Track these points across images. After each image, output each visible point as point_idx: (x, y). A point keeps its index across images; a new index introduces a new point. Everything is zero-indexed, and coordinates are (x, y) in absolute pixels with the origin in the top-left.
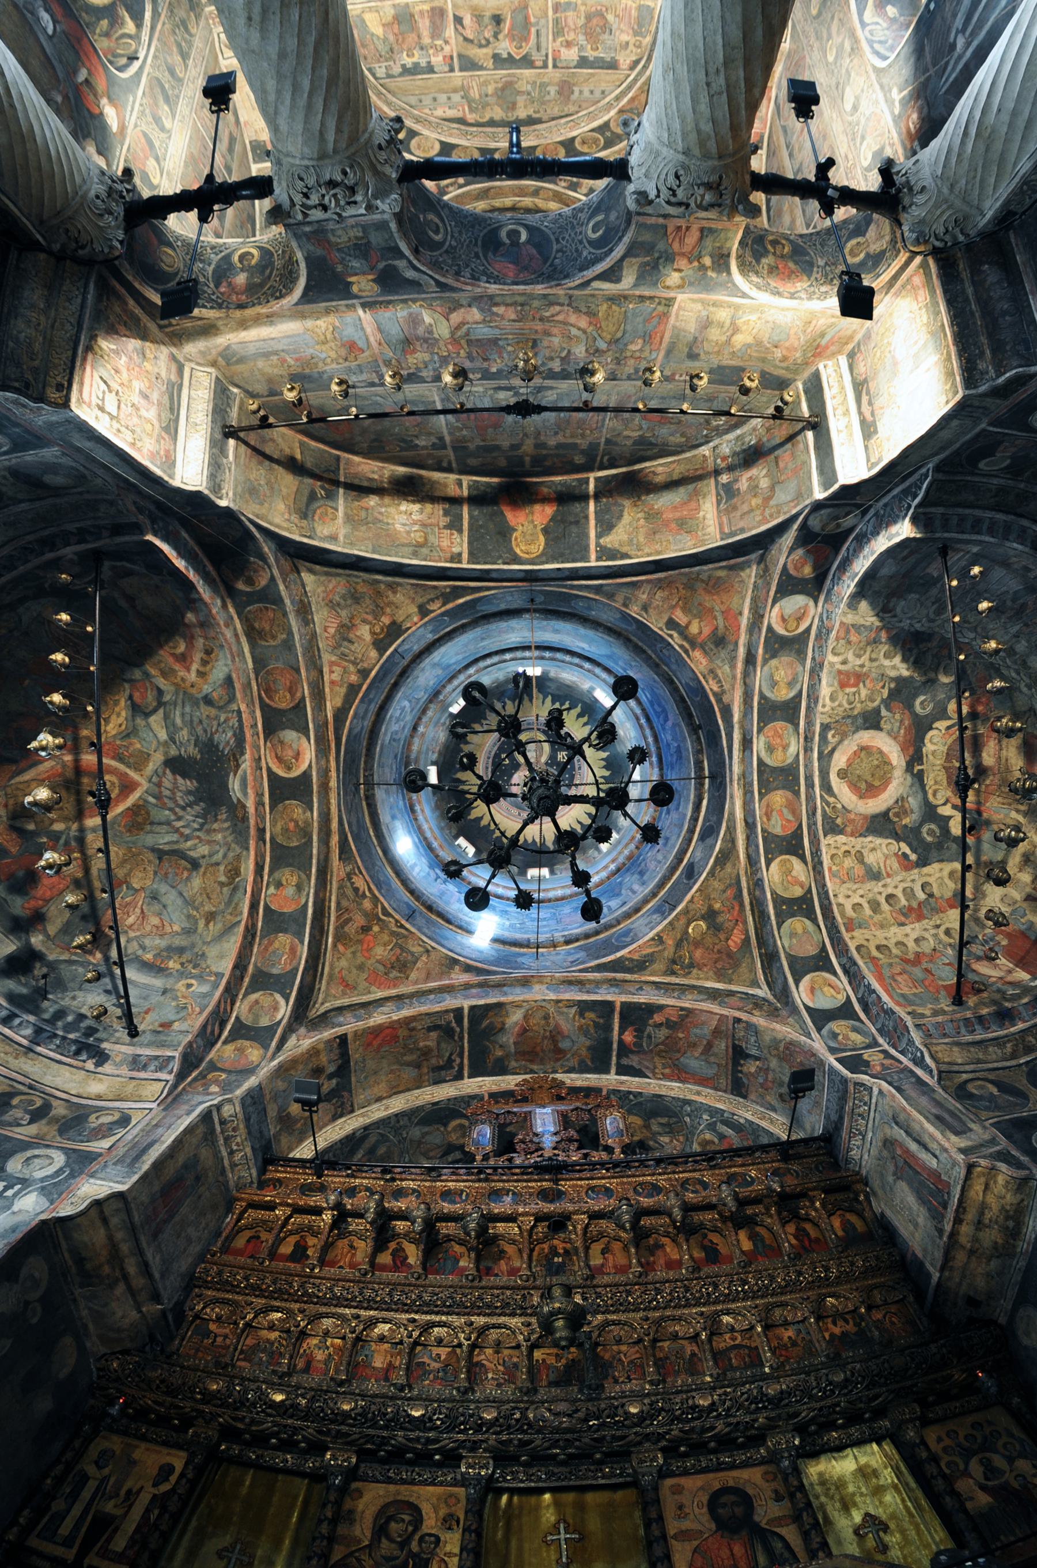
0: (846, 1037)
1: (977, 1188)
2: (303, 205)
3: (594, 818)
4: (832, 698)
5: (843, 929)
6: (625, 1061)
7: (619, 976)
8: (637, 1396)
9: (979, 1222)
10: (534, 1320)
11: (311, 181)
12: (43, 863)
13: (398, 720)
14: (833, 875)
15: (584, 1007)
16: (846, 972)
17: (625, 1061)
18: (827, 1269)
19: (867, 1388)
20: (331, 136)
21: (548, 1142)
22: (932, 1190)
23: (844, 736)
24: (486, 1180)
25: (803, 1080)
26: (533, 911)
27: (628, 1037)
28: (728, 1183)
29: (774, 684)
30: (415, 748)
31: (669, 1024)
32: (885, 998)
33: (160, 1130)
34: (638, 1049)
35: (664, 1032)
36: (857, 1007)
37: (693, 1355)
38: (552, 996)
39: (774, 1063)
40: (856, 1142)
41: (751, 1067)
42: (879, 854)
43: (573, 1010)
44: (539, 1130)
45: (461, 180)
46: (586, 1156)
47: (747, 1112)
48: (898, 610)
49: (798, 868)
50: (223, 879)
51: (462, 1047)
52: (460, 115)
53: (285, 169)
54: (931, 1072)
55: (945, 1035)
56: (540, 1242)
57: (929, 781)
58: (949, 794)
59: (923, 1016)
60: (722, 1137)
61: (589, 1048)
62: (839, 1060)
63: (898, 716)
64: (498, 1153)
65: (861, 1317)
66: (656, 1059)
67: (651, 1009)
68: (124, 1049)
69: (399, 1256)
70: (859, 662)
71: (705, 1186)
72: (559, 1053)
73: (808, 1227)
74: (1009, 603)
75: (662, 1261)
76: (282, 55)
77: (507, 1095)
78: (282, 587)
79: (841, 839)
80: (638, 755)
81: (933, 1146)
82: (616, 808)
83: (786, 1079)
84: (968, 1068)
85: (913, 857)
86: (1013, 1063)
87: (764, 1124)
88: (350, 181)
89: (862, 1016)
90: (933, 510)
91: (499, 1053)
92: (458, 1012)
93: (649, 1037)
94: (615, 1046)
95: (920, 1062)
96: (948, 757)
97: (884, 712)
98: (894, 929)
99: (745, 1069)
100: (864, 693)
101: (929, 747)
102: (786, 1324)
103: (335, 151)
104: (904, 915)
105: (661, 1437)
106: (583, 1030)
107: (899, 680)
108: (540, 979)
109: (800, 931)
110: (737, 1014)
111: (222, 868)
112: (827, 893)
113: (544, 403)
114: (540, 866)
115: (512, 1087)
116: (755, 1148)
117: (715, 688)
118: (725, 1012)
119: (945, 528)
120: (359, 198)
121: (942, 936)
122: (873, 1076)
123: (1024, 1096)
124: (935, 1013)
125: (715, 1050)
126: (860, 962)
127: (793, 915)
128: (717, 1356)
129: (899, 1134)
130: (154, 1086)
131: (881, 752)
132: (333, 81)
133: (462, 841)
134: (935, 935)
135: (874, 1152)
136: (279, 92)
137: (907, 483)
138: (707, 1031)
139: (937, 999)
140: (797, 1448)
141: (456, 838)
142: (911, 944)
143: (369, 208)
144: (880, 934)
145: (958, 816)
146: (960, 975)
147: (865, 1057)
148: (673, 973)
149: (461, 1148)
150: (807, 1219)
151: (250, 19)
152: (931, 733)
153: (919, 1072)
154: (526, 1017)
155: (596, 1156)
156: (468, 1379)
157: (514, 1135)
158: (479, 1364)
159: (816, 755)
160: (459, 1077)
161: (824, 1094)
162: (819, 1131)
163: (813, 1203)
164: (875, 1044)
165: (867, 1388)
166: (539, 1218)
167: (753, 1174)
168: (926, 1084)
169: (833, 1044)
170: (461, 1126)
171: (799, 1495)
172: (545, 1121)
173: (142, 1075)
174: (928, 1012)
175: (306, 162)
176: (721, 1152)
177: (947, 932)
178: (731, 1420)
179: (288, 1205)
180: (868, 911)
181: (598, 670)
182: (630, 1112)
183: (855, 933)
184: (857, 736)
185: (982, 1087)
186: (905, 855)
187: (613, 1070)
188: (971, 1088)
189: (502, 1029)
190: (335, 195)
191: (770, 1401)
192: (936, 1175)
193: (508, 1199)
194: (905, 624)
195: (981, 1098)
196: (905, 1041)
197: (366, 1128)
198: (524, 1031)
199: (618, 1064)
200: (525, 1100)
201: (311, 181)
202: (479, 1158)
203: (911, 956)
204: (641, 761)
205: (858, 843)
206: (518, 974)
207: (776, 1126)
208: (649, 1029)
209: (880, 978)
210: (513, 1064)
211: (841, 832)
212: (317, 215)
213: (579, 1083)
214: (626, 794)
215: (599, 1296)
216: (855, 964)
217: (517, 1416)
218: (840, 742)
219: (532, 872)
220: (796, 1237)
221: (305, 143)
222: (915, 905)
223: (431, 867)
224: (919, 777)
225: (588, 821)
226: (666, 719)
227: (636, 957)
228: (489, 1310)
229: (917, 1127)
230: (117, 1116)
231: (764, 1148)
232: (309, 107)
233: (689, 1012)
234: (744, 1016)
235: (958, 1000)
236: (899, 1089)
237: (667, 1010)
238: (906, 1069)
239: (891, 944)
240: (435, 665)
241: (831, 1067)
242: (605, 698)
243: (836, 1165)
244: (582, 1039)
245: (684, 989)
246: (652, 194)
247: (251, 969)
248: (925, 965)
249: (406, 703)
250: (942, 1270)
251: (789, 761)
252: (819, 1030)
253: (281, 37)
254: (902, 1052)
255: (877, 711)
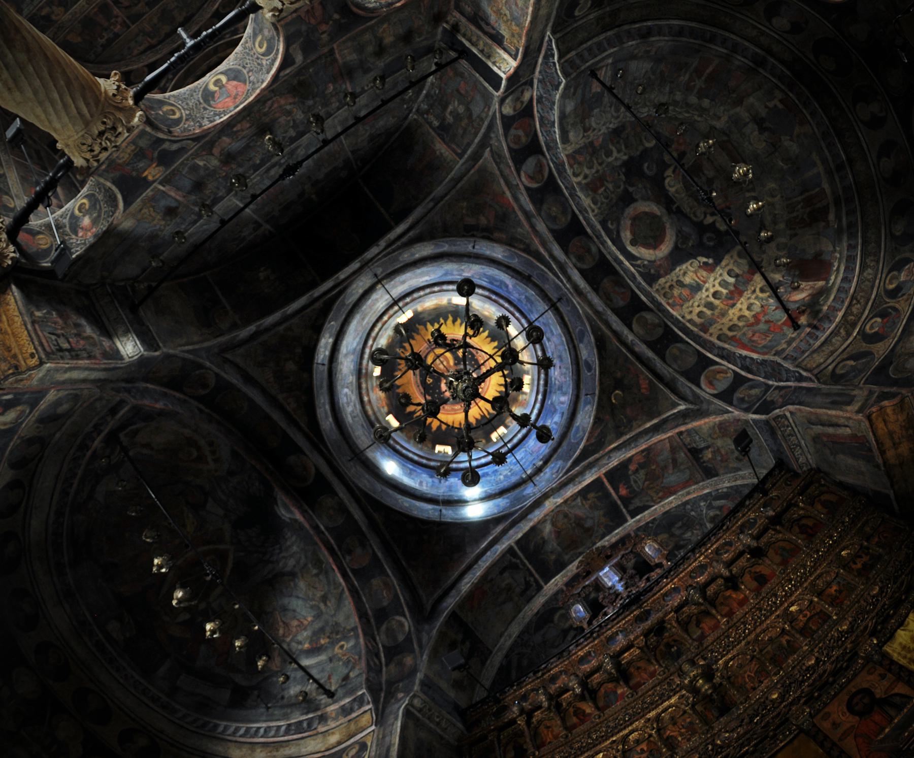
0: (749, 396)
1: (880, 425)
2: (93, 157)
3: (504, 376)
4: (595, 203)
5: (702, 334)
6: (631, 507)
7: (591, 459)
8: (770, 689)
9: (894, 444)
10: (684, 692)
11: (90, 141)
12: (208, 633)
13: (348, 404)
14: (672, 306)
15: (583, 493)
16: (722, 357)
17: (631, 507)
18: (831, 537)
19: (895, 583)
20: (85, 111)
21: (620, 587)
22: (857, 446)
23: (618, 221)
24: (598, 636)
25: (743, 440)
26: (510, 459)
27: (623, 492)
28: (742, 532)
29: (554, 219)
30: (370, 412)
31: (641, 466)
32: (755, 356)
33: (387, 739)
34: (634, 494)
35: (642, 474)
36: (743, 373)
37: (788, 642)
38: (560, 500)
39: (719, 443)
40: (798, 452)
41: (708, 455)
42: (691, 274)
43: (579, 500)
44: (610, 584)
45: (170, 76)
46: (648, 580)
47: (725, 483)
48: (594, 125)
49: (648, 316)
50: (315, 571)
51: (528, 569)
52: (147, 45)
53: (72, 146)
54: (811, 380)
55: (804, 352)
56: (655, 648)
57: (686, 209)
58: (703, 209)
59: (783, 350)
60: (720, 508)
61: (604, 515)
62: (755, 413)
63: (640, 186)
64: (594, 616)
65: (868, 548)
66: (649, 492)
67: (624, 465)
68: (332, 708)
69: (582, 716)
70: (594, 171)
71: (729, 544)
72: (589, 531)
73: (804, 521)
74: (653, 77)
75: (735, 605)
76: (35, 93)
77: (576, 579)
78: (225, 376)
79: (662, 281)
80: (503, 322)
81: (842, 421)
82: (514, 362)
83: (733, 447)
84: (829, 361)
85: (711, 261)
86: (851, 339)
87: (739, 482)
88: (110, 124)
89: (750, 376)
90: (569, 56)
91: (553, 557)
92: (510, 550)
93: (636, 482)
94: (619, 502)
95: (801, 378)
96: (687, 188)
97: (631, 189)
98: (731, 312)
99: (705, 459)
100: (610, 186)
101: (672, 190)
102: (829, 585)
103: (92, 116)
104: (730, 299)
105: (799, 698)
106: (593, 507)
107: (625, 164)
108: (546, 496)
109: (678, 353)
110: (677, 430)
111: (310, 565)
112: (677, 318)
113: (300, 159)
114: (495, 429)
115: (575, 571)
116: (742, 500)
117: (522, 247)
118: (669, 434)
119: (584, 61)
120: (120, 130)
121: (761, 295)
122: (780, 407)
123: (869, 354)
124: (789, 343)
125: (680, 460)
126: (726, 346)
127: (667, 347)
128: (804, 631)
129: (818, 429)
130: (366, 714)
131: (646, 213)
132: (69, 84)
133: (439, 448)
134: (757, 298)
135: (812, 450)
136: (45, 111)
137: (543, 52)
138: (666, 454)
139: (784, 334)
140: (877, 644)
141: (434, 448)
142: (747, 313)
143: (129, 130)
144: (725, 320)
145: (718, 218)
146: (786, 310)
147: (769, 399)
148: (622, 434)
149: (571, 627)
150: (802, 517)
151: (9, 89)
152: (667, 181)
153: (804, 384)
154: (553, 524)
155: (654, 575)
156: (668, 750)
157: (596, 599)
158: (668, 738)
159: (610, 243)
160: (539, 588)
161: (760, 439)
162: (772, 462)
163: (798, 506)
164: (769, 387)
165: (895, 583)
166: (646, 634)
167: (752, 516)
168: (813, 388)
169: (745, 406)
170: (563, 616)
171: (893, 667)
172: (609, 577)
173: (354, 715)
174: (785, 346)
175: (81, 134)
176: (726, 518)
177: (762, 290)
178: (833, 659)
179: (493, 730)
180: (708, 312)
181: (445, 287)
182: (656, 535)
183: (711, 331)
184: (626, 214)
185: (844, 366)
186: (704, 263)
187: (629, 518)
188: (839, 371)
189: (544, 542)
190: (107, 139)
191: (847, 632)
192: (854, 436)
193: (620, 637)
194: (604, 130)
195: (848, 373)
196: (784, 373)
197: (507, 656)
198: (558, 534)
199: (629, 512)
200: (588, 574)
201: (90, 141)
202: (585, 626)
203: (752, 320)
204: (508, 322)
205: (673, 276)
206: (528, 503)
207: (746, 478)
208: (632, 477)
209: (744, 347)
210: (566, 557)
211: (659, 276)
212: (104, 156)
213: (614, 540)
214: (514, 350)
215: (712, 651)
216: (724, 349)
217: (710, 747)
218: (619, 224)
219: (494, 436)
220: (802, 533)
221: (74, 125)
222: (732, 288)
223: (432, 477)
224: (679, 211)
225: (502, 381)
226: (507, 286)
227: (593, 441)
228: (654, 705)
229: (826, 418)
230: (357, 747)
231: (749, 496)
232: (65, 106)
233: (648, 450)
234: (683, 428)
235: (796, 326)
236: (800, 404)
237: (635, 458)
238: (796, 387)
239: (735, 321)
240: (346, 355)
241: (754, 420)
242: (461, 301)
243: (796, 475)
244: (597, 513)
245: (635, 439)
246: (280, 6)
247: (369, 612)
248: (763, 319)
249: (346, 390)
250: (892, 486)
251: (597, 257)
252: (731, 404)
253: (30, 85)
254: (787, 381)
255: (626, 190)
